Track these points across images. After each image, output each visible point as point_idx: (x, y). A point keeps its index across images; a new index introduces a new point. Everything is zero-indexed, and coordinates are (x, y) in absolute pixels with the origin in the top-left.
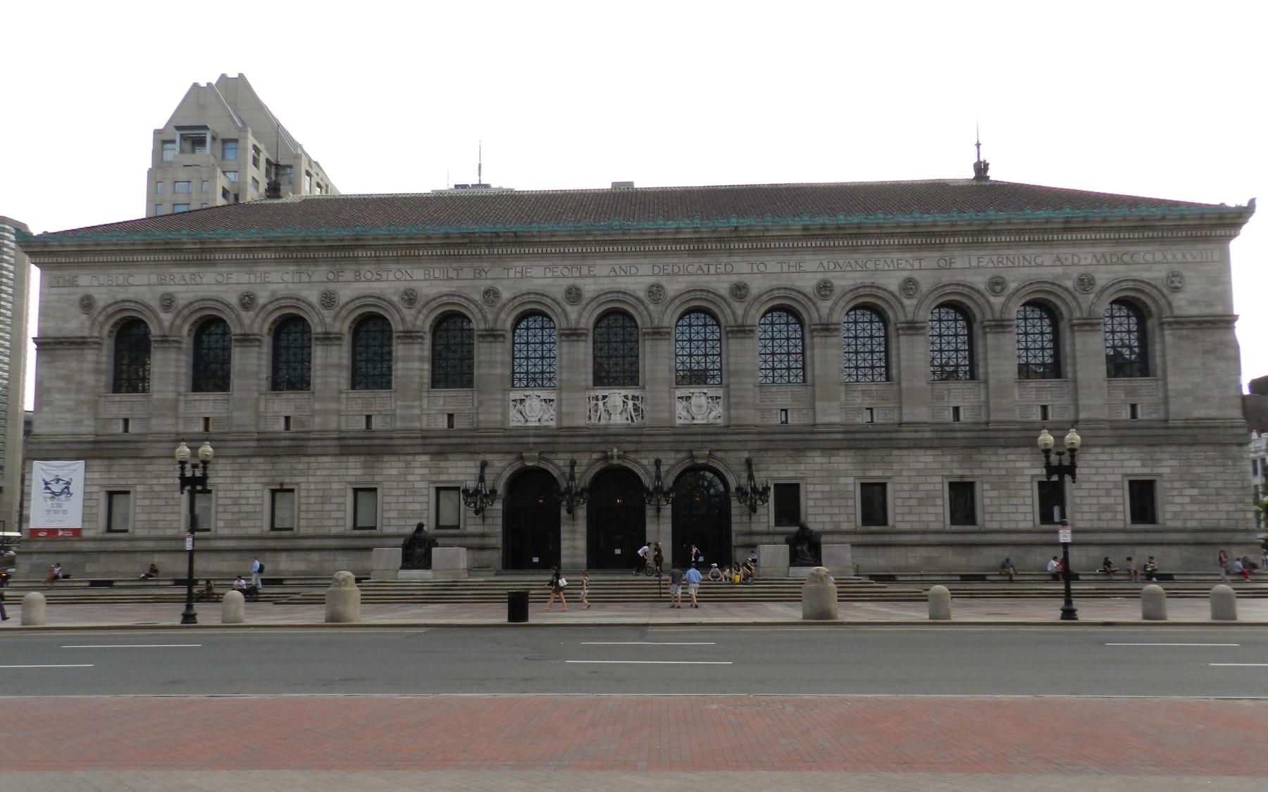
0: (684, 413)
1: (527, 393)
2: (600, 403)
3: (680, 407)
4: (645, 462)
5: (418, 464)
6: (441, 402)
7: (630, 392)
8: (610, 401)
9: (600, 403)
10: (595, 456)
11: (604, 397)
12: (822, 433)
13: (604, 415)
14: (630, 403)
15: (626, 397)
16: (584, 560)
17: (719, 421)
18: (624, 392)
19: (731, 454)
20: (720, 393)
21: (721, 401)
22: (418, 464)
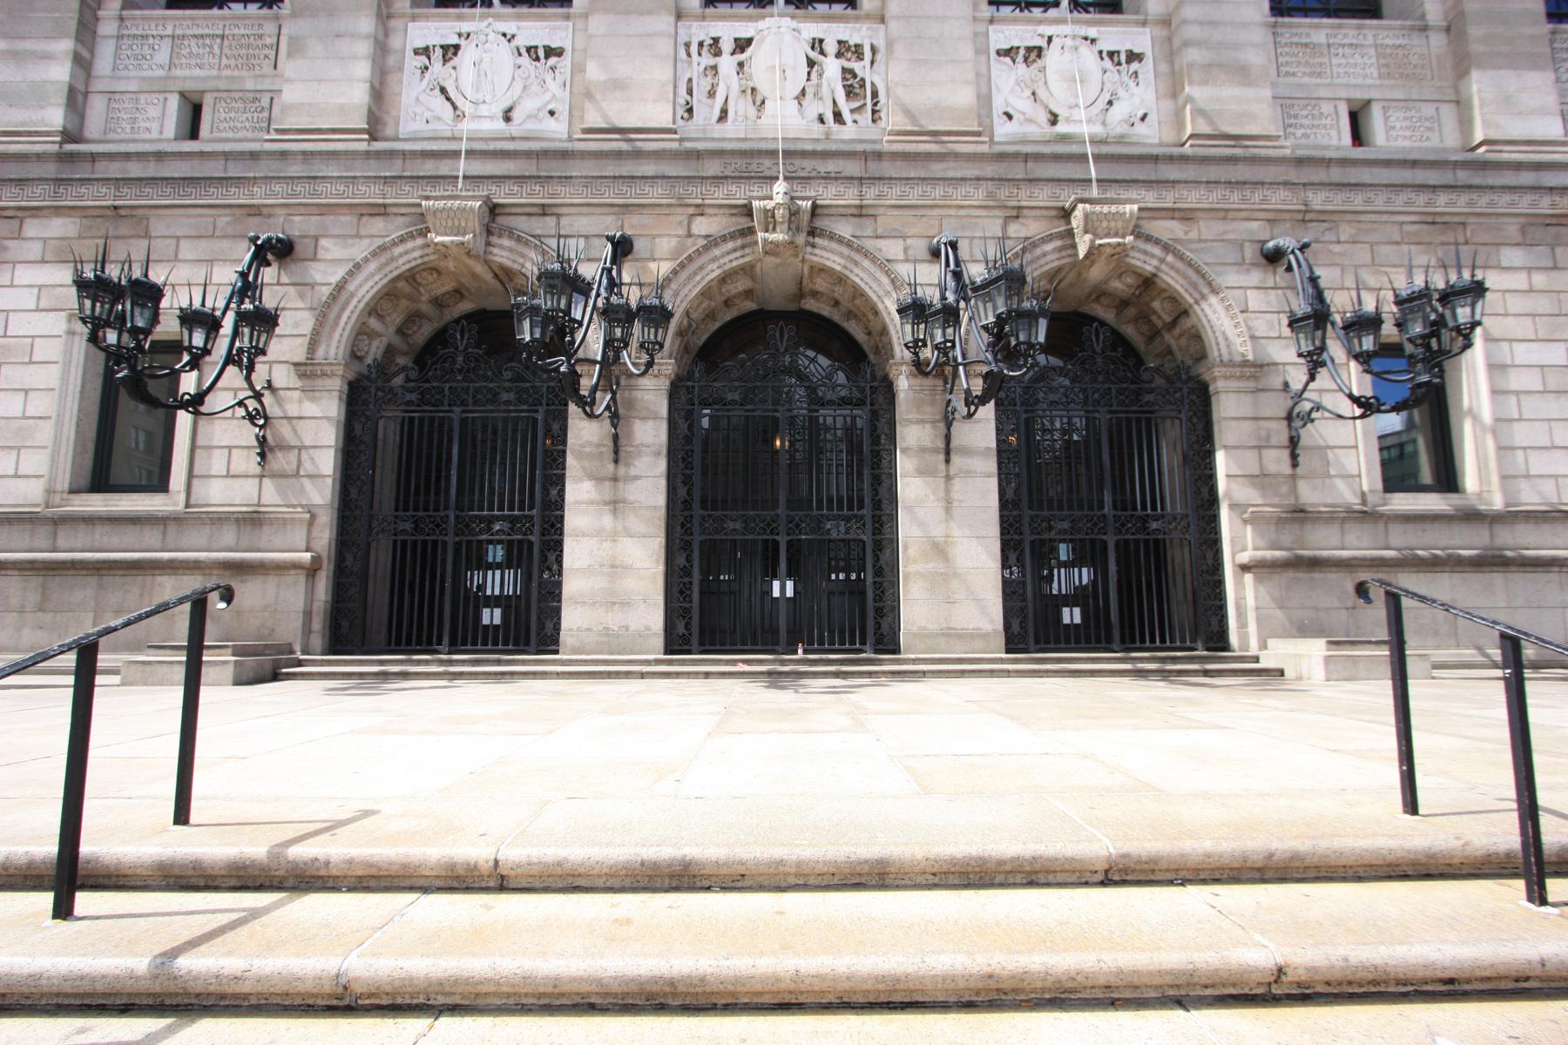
0: (1021, 103)
1: (465, 27)
2: (727, 63)
3: (1008, 82)
4: (892, 249)
5: (34, 250)
6: (163, 55)
7: (833, 33)
8: (757, 57)
9: (727, 63)
10: (702, 226)
11: (742, 45)
12: (1518, 166)
13: (740, 108)
14: (832, 67)
15: (817, 44)
16: (654, 619)
17: (1141, 129)
18: (811, 30)
19: (1208, 228)
20: (1141, 39)
21: (1146, 68)
22: (34, 250)
